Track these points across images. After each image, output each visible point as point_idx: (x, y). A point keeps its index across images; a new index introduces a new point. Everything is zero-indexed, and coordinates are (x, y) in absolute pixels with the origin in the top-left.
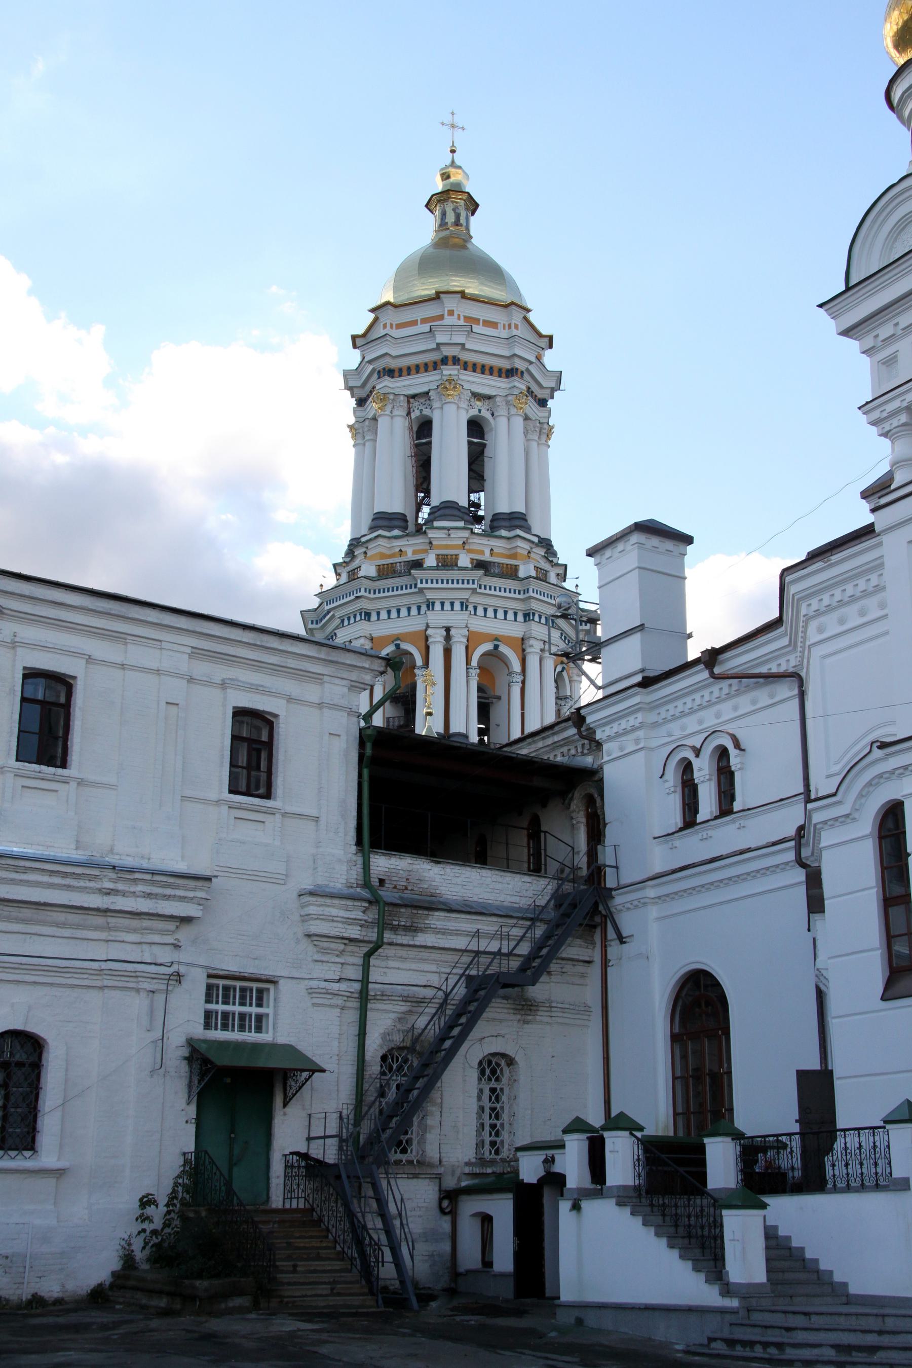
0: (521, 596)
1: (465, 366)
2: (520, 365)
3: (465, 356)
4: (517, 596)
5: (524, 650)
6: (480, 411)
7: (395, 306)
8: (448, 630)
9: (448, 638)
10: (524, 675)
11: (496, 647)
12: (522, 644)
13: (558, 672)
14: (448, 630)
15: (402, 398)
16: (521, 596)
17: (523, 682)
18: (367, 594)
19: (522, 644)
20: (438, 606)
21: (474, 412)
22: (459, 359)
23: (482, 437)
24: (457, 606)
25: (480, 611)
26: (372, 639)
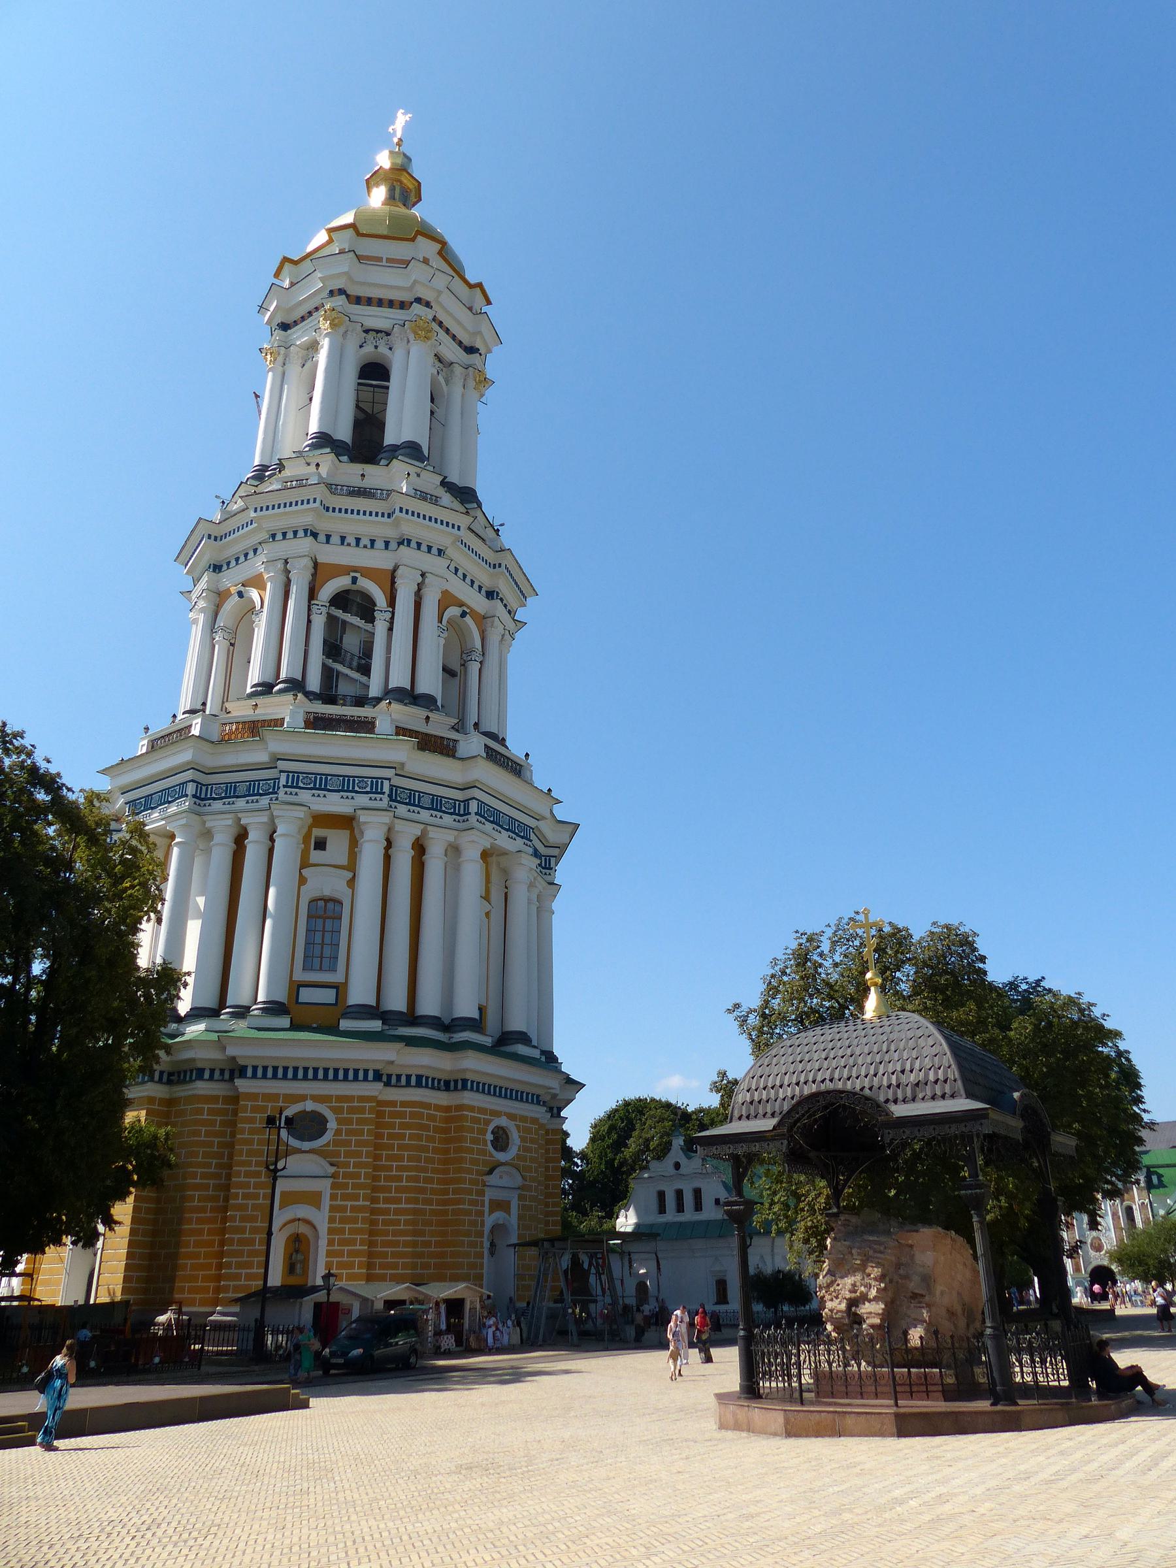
1: (358, 300)
2: (427, 295)
3: (353, 291)
5: (393, 583)
6: (376, 347)
8: (286, 562)
10: (393, 613)
11: (354, 580)
14: (286, 562)
21: (369, 348)
22: (345, 291)
23: (388, 380)
24: (301, 533)
25: (335, 539)
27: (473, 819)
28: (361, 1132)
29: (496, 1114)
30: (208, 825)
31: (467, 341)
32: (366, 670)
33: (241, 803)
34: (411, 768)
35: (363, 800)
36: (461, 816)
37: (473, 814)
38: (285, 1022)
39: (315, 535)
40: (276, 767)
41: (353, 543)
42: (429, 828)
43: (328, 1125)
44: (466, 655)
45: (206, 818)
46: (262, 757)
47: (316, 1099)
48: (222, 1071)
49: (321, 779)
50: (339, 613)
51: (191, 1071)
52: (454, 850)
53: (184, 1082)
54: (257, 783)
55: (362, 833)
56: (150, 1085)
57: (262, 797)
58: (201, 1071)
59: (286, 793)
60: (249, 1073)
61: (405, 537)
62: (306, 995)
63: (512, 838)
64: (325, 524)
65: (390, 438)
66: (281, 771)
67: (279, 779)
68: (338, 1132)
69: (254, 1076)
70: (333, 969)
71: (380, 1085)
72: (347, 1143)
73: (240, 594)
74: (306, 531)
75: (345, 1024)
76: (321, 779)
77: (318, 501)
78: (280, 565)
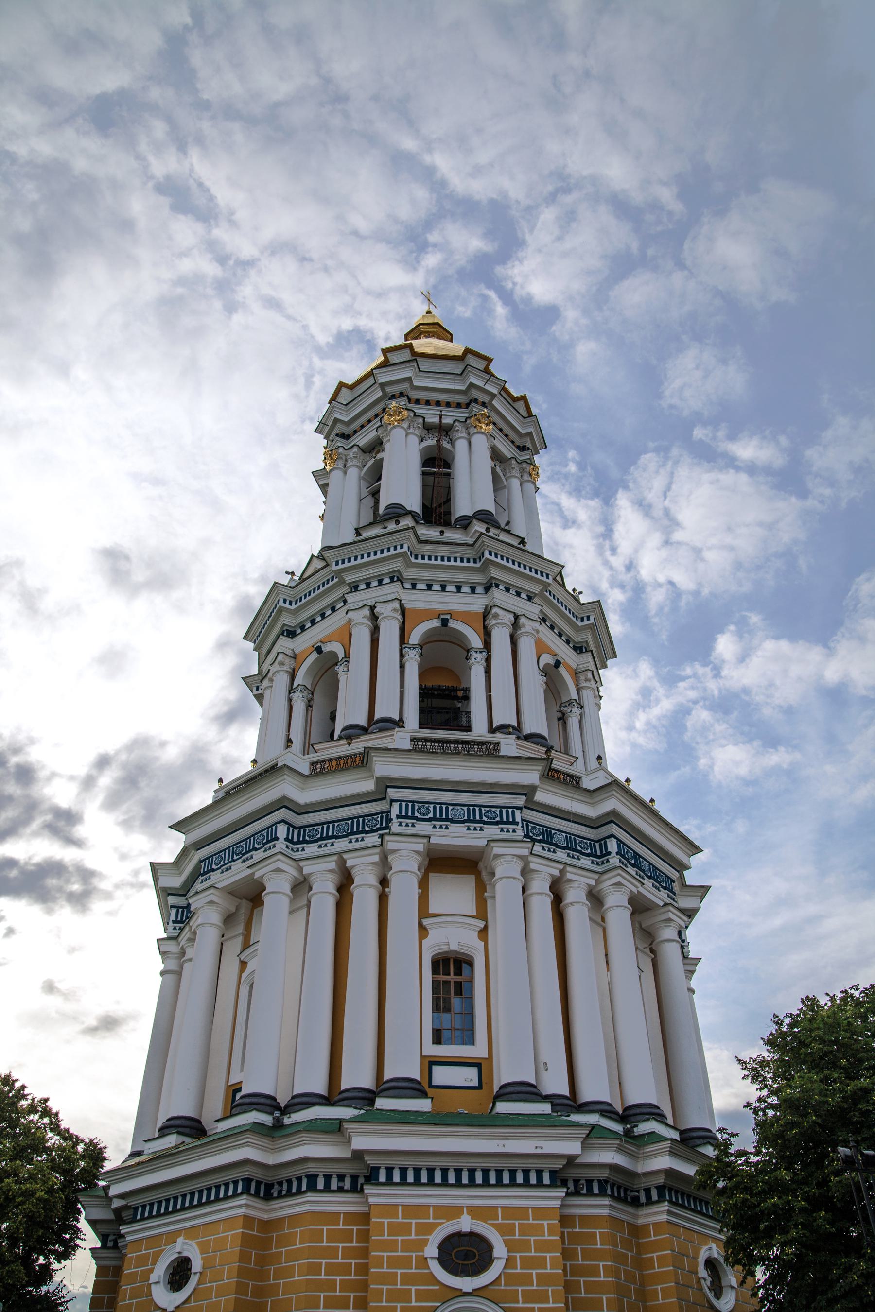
0: (478, 565)
3: (414, 395)
4: (472, 564)
7: (352, 387)
8: (372, 608)
9: (374, 618)
11: (445, 622)
12: (484, 621)
14: (372, 608)
15: (355, 449)
16: (478, 565)
17: (488, 660)
18: (287, 605)
19: (484, 621)
20: (362, 586)
24: (386, 580)
26: (295, 657)
27: (615, 860)
28: (540, 1263)
30: (306, 871)
31: (519, 442)
33: (342, 845)
34: (541, 797)
36: (599, 857)
37: (614, 854)
38: (423, 1105)
39: (401, 580)
40: (384, 799)
41: (440, 589)
42: (569, 869)
43: (495, 1254)
45: (302, 864)
46: (369, 786)
47: (476, 1212)
48: (341, 1178)
49: (441, 808)
51: (299, 1179)
52: (595, 899)
53: (289, 1194)
54: (361, 819)
55: (493, 874)
56: (243, 1200)
57: (368, 835)
58: (312, 1179)
59: (400, 825)
60: (382, 1178)
61: (494, 581)
62: (442, 1075)
63: (656, 887)
64: (408, 574)
65: (462, 507)
66: (392, 801)
67: (390, 811)
68: (510, 1262)
69: (390, 1182)
70: (470, 1040)
71: (561, 1192)
72: (526, 1279)
73: (319, 650)
74: (392, 579)
75: (502, 1107)
76: (441, 808)
77: (405, 548)
78: (366, 612)
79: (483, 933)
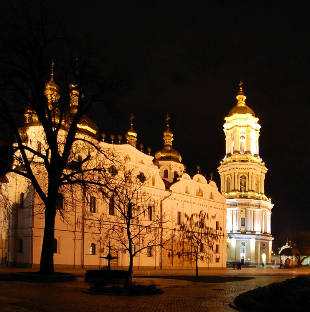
10: (249, 179)
13: (257, 178)
29: (264, 242)
31: (256, 129)
32: (245, 186)
35: (247, 206)
38: (240, 233)
44: (258, 182)
47: (244, 241)
50: (241, 179)
62: (242, 229)
75: (247, 233)
79: (246, 216)
